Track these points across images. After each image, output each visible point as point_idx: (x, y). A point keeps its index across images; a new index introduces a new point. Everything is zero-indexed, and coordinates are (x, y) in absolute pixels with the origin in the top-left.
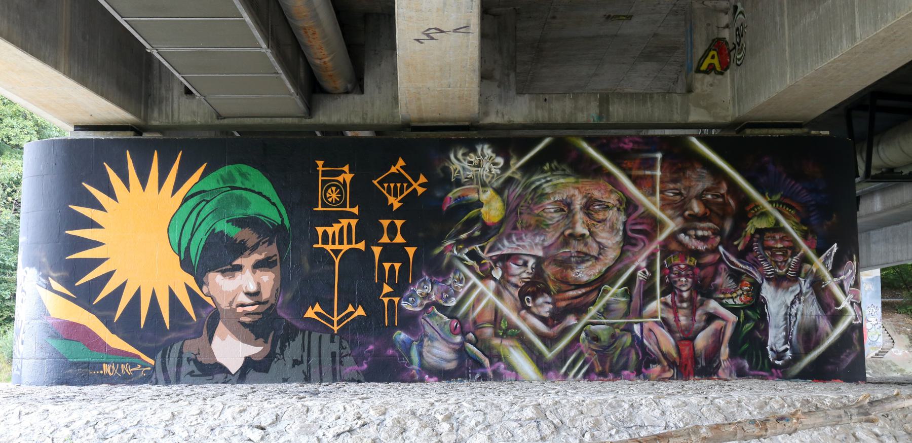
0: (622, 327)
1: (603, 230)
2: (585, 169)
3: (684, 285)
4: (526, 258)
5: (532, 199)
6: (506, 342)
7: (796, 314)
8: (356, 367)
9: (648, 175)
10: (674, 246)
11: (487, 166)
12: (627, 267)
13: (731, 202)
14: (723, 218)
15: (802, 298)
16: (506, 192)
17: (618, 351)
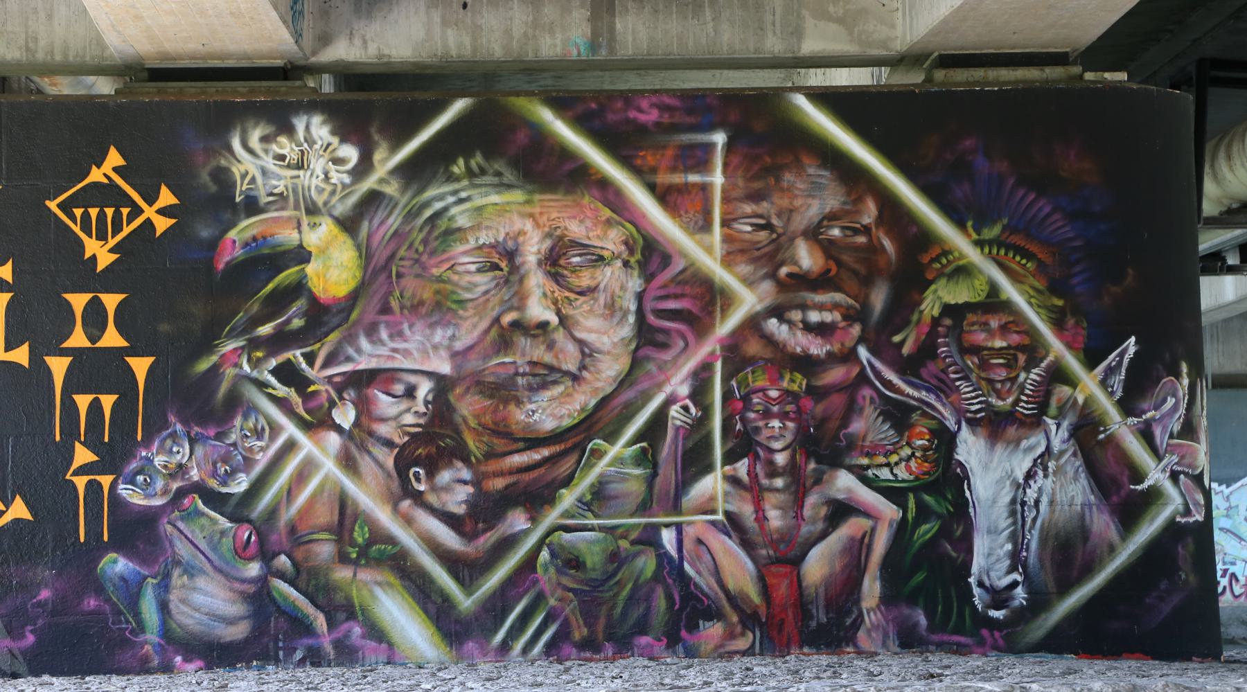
0: (634, 535)
1: (591, 311)
2: (547, 170)
3: (778, 436)
4: (412, 379)
5: (425, 242)
6: (365, 575)
7: (1037, 502)
8: (7, 642)
9: (694, 185)
10: (753, 348)
11: (318, 165)
12: (646, 398)
13: (887, 244)
14: (867, 282)
15: (1051, 465)
16: (365, 225)
17: (625, 593)
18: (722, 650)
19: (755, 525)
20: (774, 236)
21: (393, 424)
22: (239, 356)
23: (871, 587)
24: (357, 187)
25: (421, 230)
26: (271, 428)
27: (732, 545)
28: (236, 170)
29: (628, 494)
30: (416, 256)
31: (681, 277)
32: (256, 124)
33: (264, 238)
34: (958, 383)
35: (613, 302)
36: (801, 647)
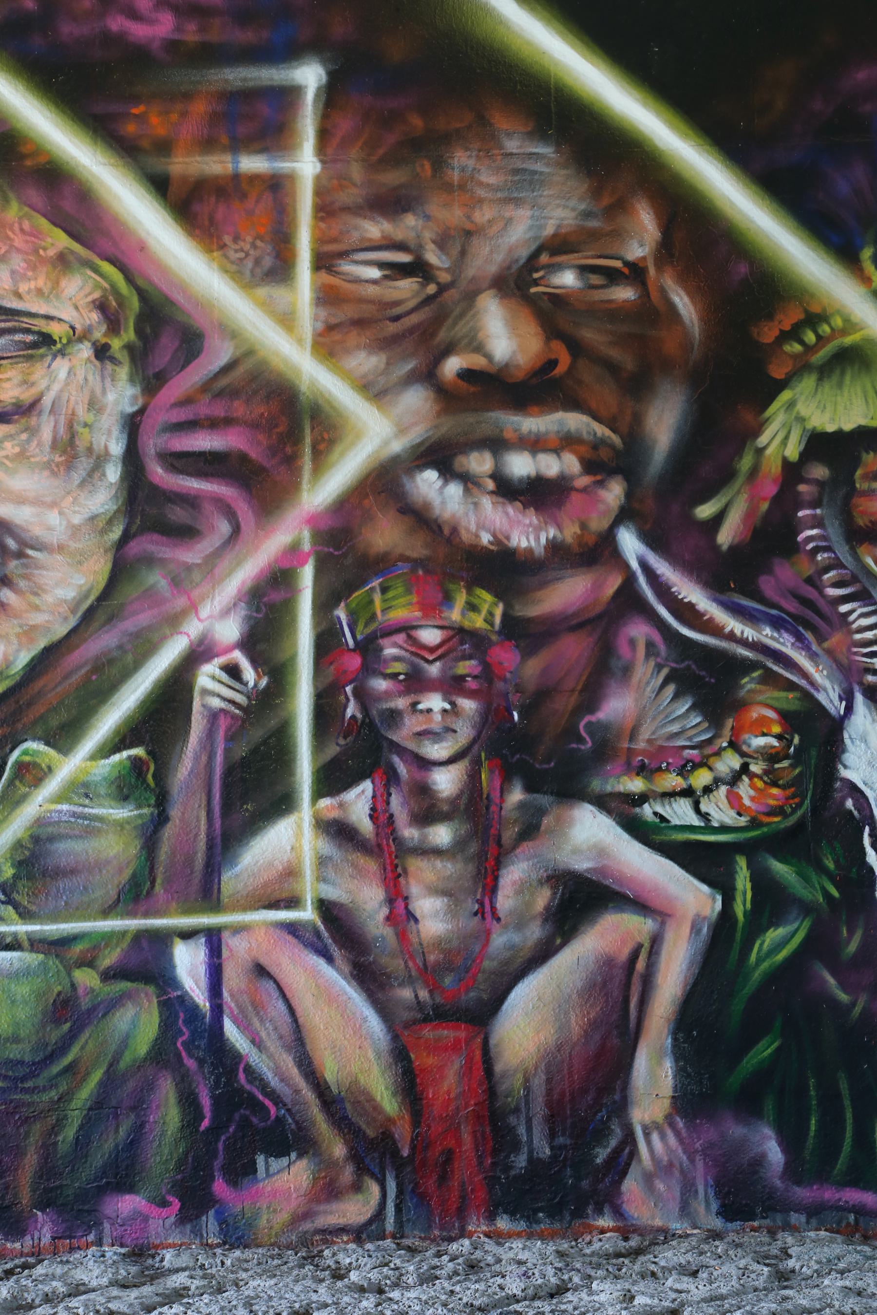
0: (109, 959)
1: (22, 456)
3: (440, 730)
9: (254, 178)
10: (385, 535)
12: (144, 647)
13: (683, 302)
14: (638, 386)
17: (86, 1092)
18: (307, 1226)
19: (388, 932)
20: (432, 289)
23: (652, 1075)
27: (335, 978)
29: (99, 865)
31: (223, 382)
34: (844, 608)
35: (73, 436)
36: (491, 1217)
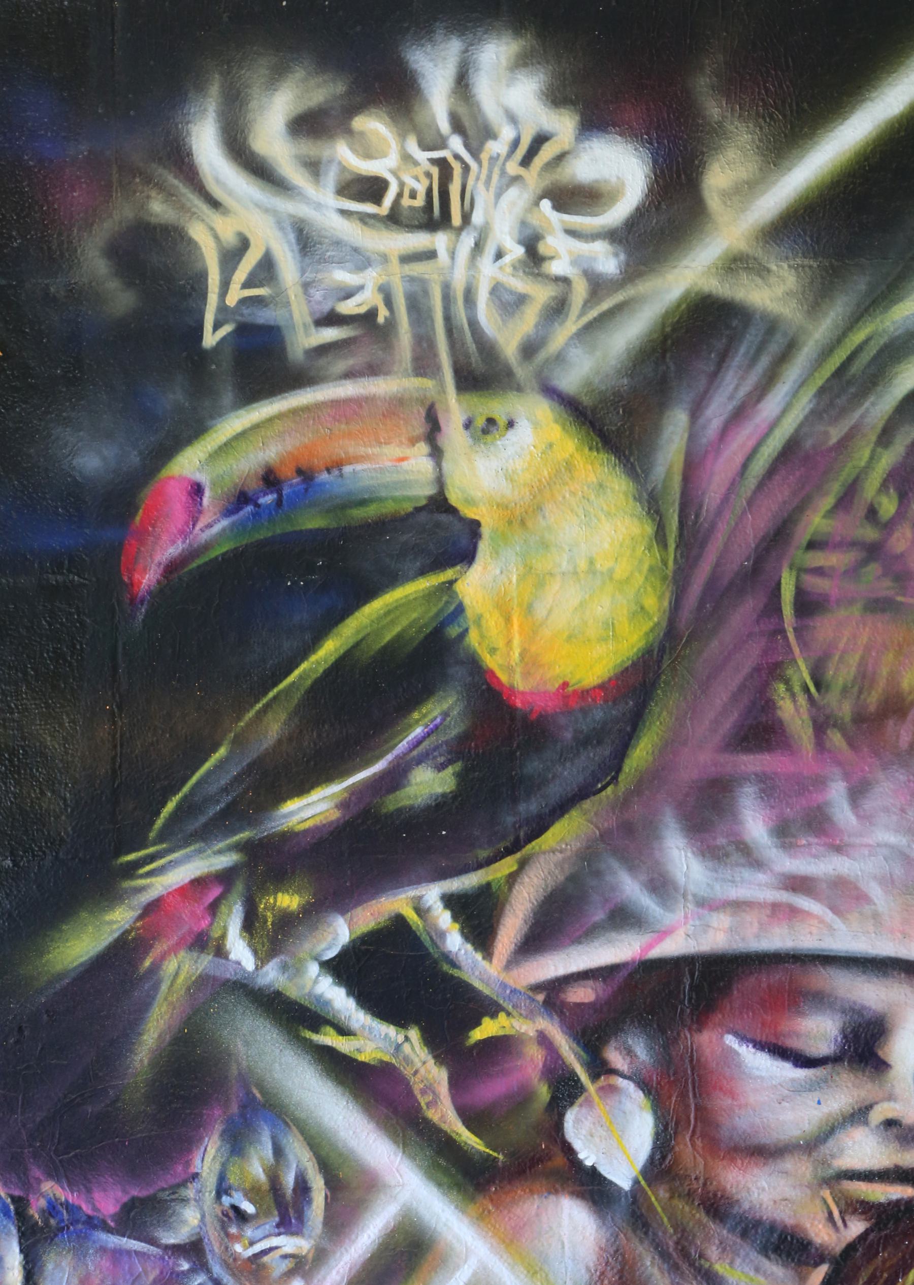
4: (871, 993)
11: (502, 210)
21: (801, 1168)
22: (213, 908)
24: (643, 287)
25: (886, 436)
26: (334, 1184)
28: (206, 236)
30: (870, 534)
32: (278, 74)
33: (306, 475)
